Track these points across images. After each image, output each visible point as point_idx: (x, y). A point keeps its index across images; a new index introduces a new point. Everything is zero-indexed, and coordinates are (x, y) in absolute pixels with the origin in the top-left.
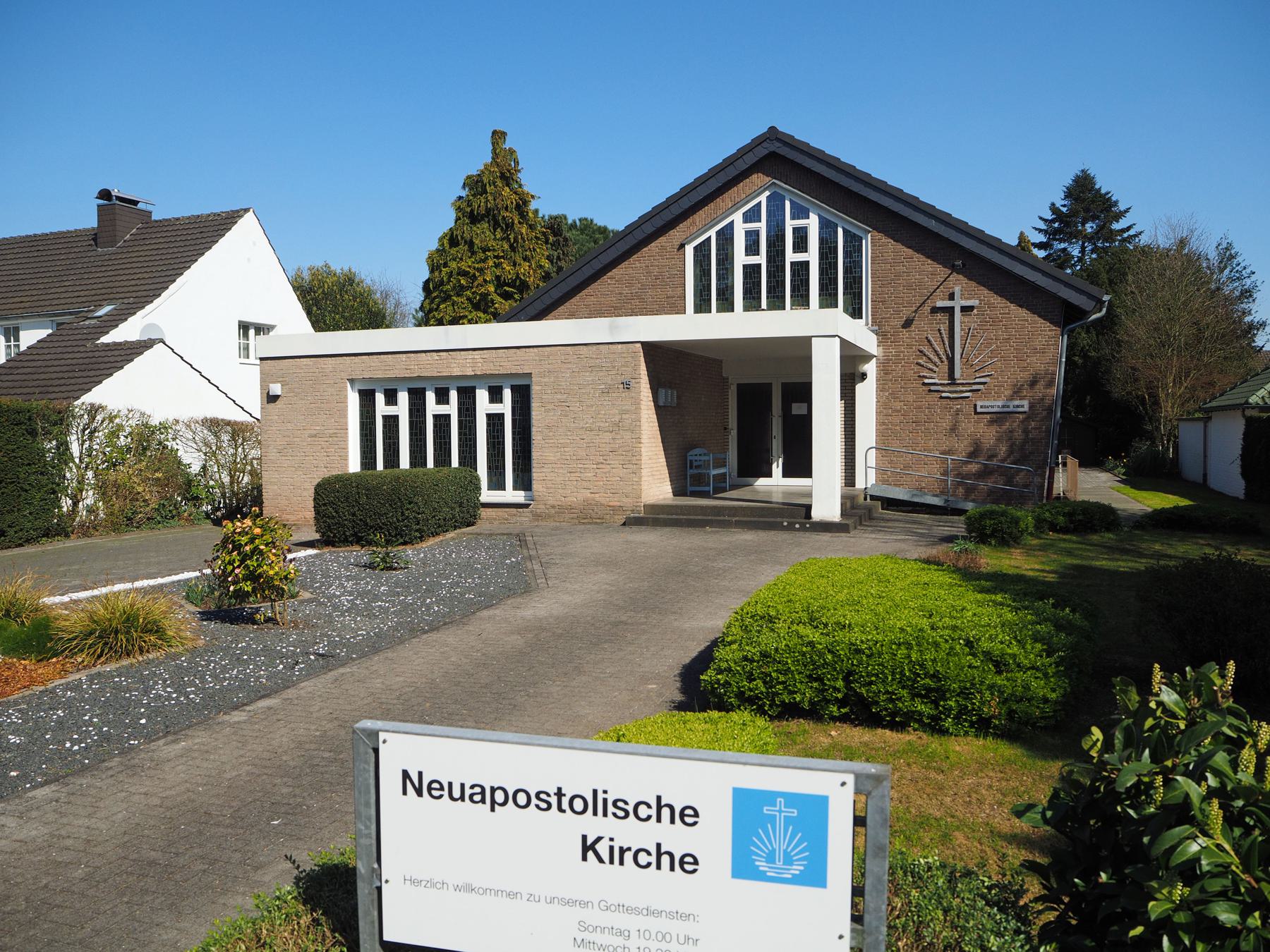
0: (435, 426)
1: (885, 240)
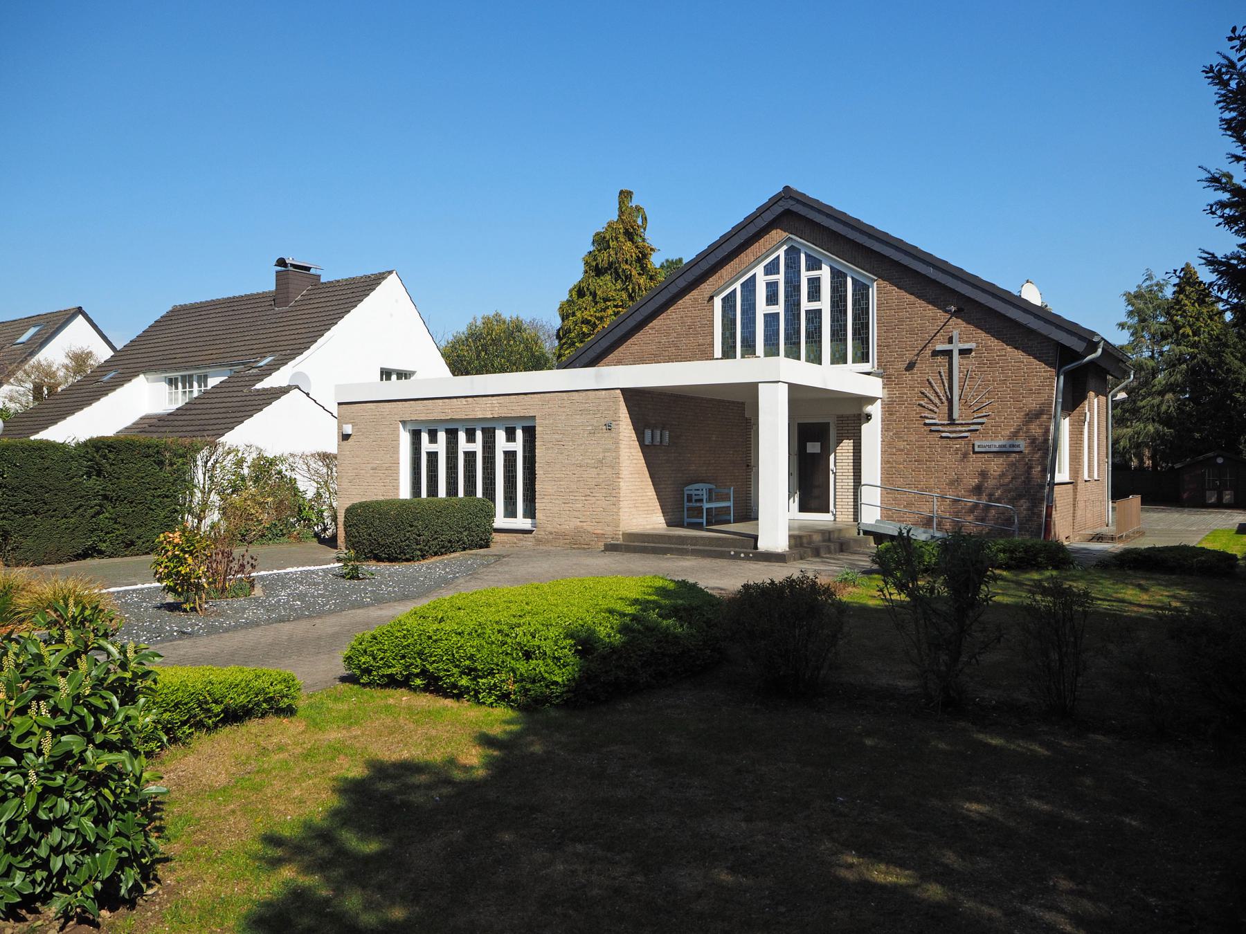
0: (465, 461)
1: (890, 287)
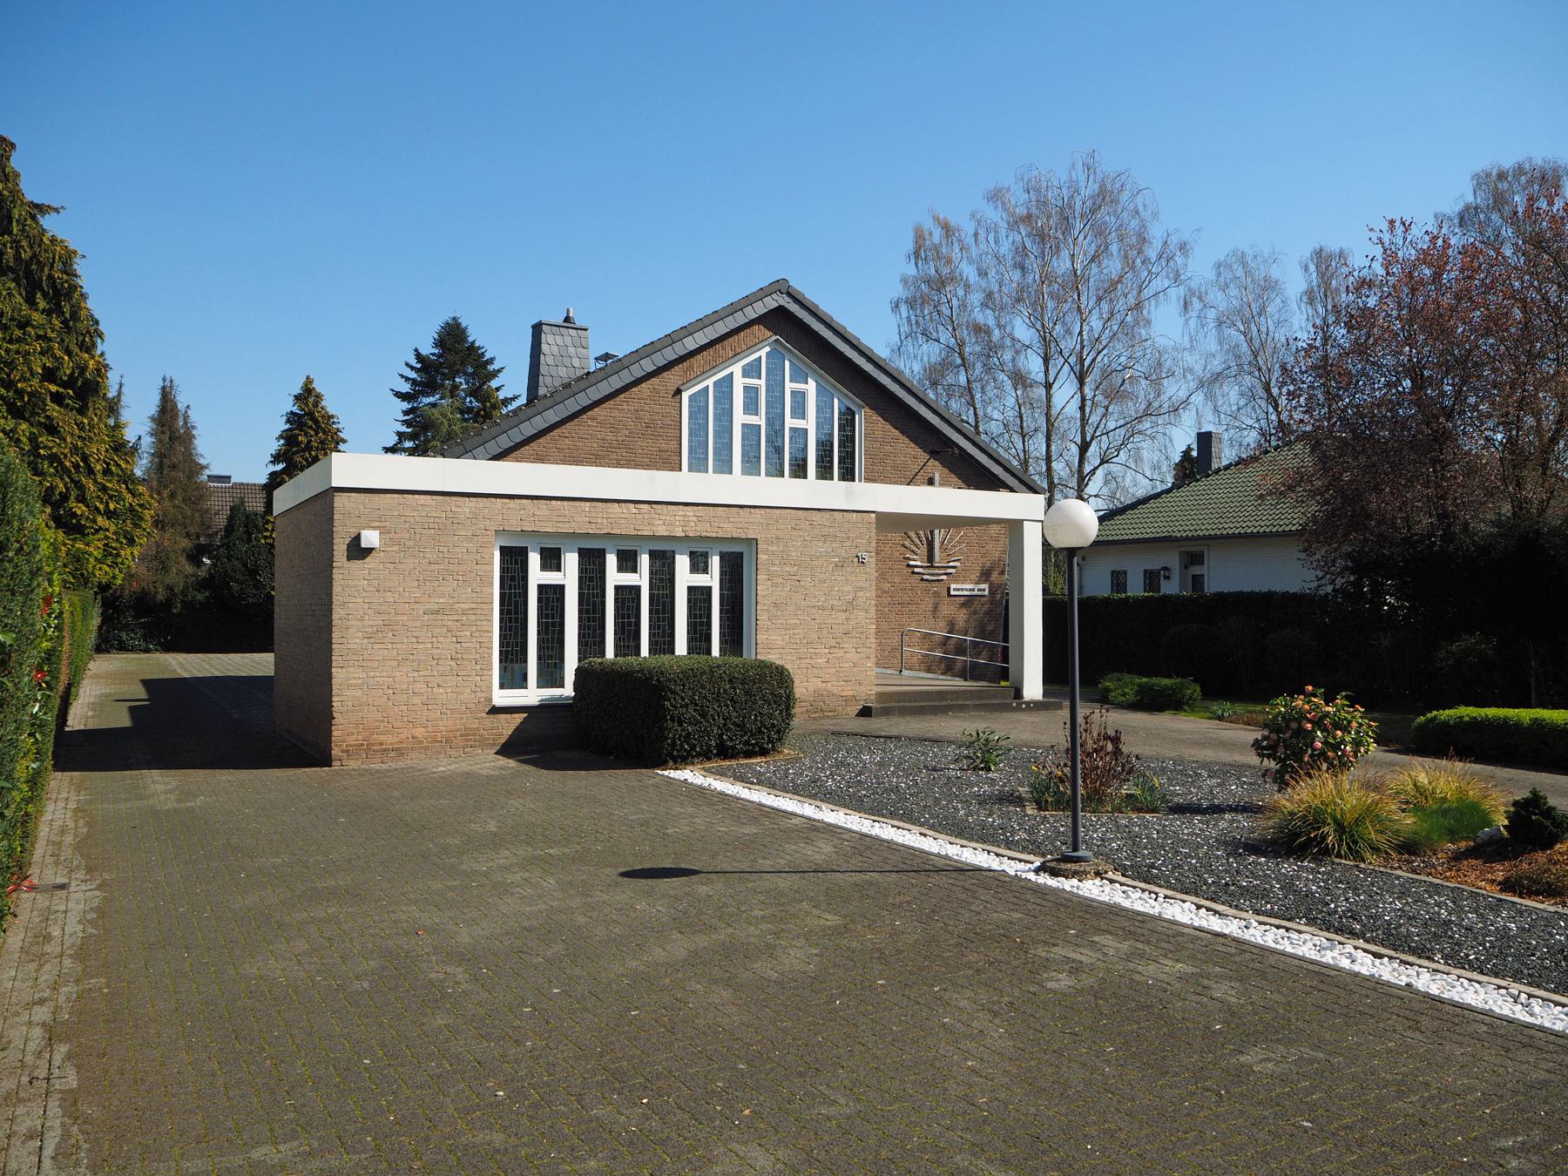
1: (876, 418)
